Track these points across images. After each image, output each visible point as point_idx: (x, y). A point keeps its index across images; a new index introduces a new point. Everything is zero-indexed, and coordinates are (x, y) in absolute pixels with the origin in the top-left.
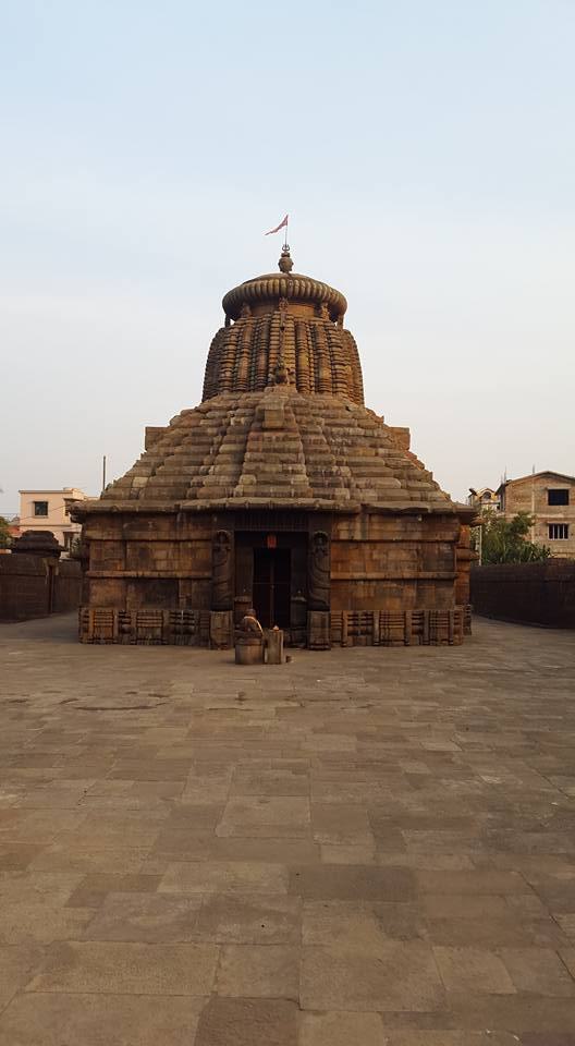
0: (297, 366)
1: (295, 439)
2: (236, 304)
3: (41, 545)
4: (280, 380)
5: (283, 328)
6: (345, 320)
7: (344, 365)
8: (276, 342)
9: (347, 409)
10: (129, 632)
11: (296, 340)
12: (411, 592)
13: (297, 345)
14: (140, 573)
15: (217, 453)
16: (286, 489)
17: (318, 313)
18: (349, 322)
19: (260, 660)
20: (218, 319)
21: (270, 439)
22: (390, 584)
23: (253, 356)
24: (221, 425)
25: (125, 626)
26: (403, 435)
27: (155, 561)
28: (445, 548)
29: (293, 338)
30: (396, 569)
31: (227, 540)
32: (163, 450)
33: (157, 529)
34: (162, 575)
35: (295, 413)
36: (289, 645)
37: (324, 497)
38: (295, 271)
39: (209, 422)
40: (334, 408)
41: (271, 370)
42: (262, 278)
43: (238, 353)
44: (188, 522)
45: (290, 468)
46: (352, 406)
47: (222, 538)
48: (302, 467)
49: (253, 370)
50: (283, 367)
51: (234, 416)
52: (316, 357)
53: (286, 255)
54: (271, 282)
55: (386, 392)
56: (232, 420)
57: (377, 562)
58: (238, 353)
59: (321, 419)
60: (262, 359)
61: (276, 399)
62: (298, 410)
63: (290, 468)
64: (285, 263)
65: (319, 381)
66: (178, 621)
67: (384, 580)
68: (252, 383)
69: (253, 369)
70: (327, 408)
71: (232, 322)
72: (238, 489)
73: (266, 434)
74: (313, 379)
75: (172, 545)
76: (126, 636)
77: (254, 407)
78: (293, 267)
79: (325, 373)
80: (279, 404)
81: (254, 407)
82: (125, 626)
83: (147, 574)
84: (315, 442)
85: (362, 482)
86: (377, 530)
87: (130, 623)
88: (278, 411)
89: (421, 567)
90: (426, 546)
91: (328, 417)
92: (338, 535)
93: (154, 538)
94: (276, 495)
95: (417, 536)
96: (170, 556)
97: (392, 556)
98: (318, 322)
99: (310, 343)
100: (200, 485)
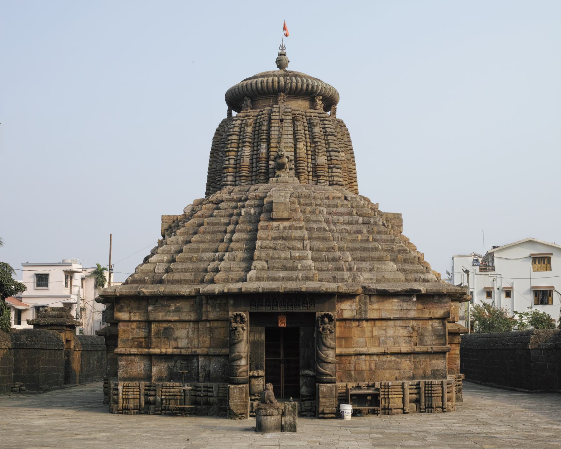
0: (296, 153)
1: (301, 228)
2: (236, 99)
3: (59, 321)
4: (281, 167)
5: (282, 120)
6: (337, 110)
7: (339, 152)
8: (277, 133)
9: (346, 198)
10: (154, 403)
11: (294, 130)
12: (406, 364)
13: (295, 134)
14: (164, 350)
15: (231, 241)
16: (294, 274)
17: (313, 106)
18: (342, 111)
20: (221, 111)
22: (389, 358)
24: (231, 215)
25: (151, 398)
26: (395, 220)
27: (176, 339)
28: (437, 324)
29: (292, 129)
30: (394, 344)
31: (242, 320)
32: (181, 239)
33: (178, 310)
34: (184, 351)
35: (299, 204)
36: (302, 414)
39: (222, 213)
40: (334, 198)
41: (272, 158)
42: (263, 76)
43: (241, 142)
44: (207, 303)
45: (297, 255)
46: (350, 195)
47: (239, 319)
48: (309, 254)
49: (255, 158)
50: (283, 156)
51: (243, 207)
52: (314, 145)
54: (270, 79)
55: (377, 180)
56: (243, 211)
57: (378, 338)
58: (241, 142)
59: (322, 208)
60: (263, 148)
61: (283, 190)
62: (302, 201)
63: (297, 255)
64: (281, 63)
65: (315, 167)
66: (198, 393)
67: (384, 354)
68: (254, 169)
69: (255, 157)
70: (328, 198)
71: (234, 114)
72: (252, 274)
73: (275, 224)
74: (310, 165)
75: (191, 324)
76: (150, 407)
77: (262, 199)
78: (289, 64)
79: (322, 160)
80: (286, 197)
81: (262, 199)
82: (151, 398)
83: (170, 351)
84: (319, 230)
85: (364, 265)
86: (376, 309)
87: (155, 395)
88: (285, 203)
89: (417, 341)
90: (420, 323)
91: (329, 206)
92: (342, 313)
93: (177, 318)
94: (283, 279)
95: (412, 314)
96: (191, 335)
97: (391, 332)
98: (313, 113)
99: (307, 132)
100: (217, 270)
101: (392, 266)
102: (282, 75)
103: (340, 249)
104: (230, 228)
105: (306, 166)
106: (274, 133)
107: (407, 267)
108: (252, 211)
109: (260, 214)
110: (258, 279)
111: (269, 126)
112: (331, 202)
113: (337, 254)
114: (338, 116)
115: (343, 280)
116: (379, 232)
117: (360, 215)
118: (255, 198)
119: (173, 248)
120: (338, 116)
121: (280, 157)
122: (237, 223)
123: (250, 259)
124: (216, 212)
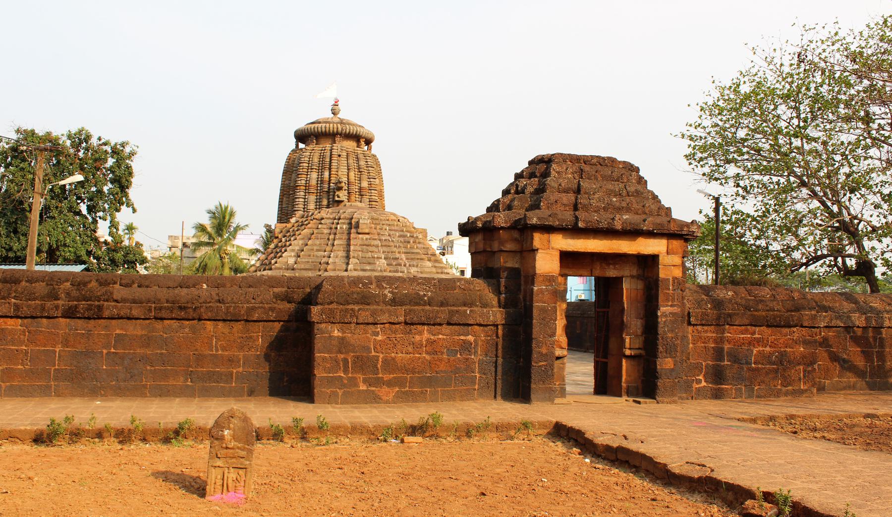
18: (375, 147)
20: (291, 143)
21: (362, 239)
23: (321, 170)
32: (301, 242)
37: (394, 272)
38: (341, 115)
39: (325, 226)
42: (326, 122)
53: (336, 104)
56: (339, 227)
58: (310, 168)
60: (327, 174)
65: (360, 189)
71: (301, 146)
73: (360, 236)
79: (365, 184)
98: (359, 151)
101: (429, 264)
102: (337, 123)
103: (399, 253)
104: (332, 237)
105: (355, 188)
106: (334, 164)
107: (437, 265)
108: (344, 227)
109: (350, 228)
110: (355, 270)
111: (331, 160)
112: (391, 223)
113: (398, 255)
114: (373, 151)
115: (403, 272)
116: (419, 243)
117: (408, 231)
118: (344, 219)
119: (297, 248)
120: (373, 151)
121: (340, 182)
122: (335, 234)
123: (348, 257)
124: (320, 226)
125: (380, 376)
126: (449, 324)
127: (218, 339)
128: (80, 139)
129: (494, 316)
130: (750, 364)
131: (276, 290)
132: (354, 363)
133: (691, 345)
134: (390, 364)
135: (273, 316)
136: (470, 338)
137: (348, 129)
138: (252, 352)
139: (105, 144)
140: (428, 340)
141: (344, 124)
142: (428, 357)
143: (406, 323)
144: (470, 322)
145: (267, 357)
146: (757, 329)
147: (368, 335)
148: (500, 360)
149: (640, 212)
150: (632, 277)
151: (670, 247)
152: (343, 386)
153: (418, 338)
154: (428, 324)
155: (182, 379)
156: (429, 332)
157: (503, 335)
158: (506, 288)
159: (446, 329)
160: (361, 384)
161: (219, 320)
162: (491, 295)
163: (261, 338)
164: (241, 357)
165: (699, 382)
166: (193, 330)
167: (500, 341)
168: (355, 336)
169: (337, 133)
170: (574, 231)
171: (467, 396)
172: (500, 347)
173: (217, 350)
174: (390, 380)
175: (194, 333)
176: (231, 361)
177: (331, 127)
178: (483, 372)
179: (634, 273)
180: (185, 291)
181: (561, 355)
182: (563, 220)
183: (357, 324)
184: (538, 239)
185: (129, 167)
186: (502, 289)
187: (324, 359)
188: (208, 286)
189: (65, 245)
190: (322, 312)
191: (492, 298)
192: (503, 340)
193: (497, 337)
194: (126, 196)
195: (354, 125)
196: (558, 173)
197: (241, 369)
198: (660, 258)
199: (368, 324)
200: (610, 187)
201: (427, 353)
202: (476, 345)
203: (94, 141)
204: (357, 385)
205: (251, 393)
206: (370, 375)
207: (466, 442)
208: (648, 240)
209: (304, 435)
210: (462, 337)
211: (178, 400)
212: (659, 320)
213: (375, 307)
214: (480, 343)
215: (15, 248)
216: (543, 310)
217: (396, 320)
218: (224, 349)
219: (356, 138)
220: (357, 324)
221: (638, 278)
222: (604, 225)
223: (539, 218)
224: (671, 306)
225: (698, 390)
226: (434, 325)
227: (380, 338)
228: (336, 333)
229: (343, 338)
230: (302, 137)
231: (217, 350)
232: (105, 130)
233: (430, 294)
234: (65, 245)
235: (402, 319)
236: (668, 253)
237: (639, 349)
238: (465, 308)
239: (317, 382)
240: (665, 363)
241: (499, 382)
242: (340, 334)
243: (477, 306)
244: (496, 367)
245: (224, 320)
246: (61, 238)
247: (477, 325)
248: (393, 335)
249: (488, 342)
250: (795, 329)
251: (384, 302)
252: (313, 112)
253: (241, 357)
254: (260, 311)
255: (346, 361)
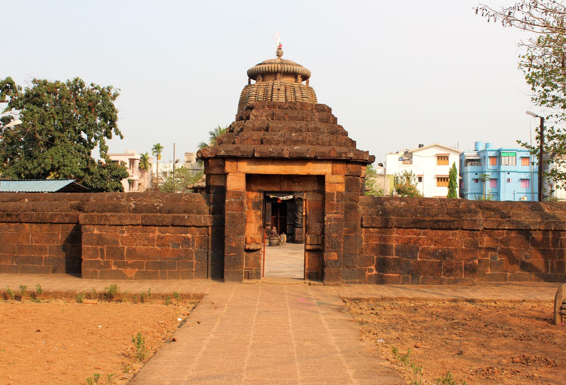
2: (252, 75)
5: (279, 90)
18: (312, 83)
19: (278, 245)
36: (288, 242)
42: (269, 63)
71: (253, 82)
98: (296, 85)
102: (279, 63)
111: (272, 93)
114: (310, 85)
120: (310, 85)
125: (126, 260)
126: (173, 225)
127: (33, 235)
128: (77, 85)
129: (205, 220)
130: (416, 258)
131: (72, 202)
132: (108, 251)
133: (364, 243)
134: (132, 253)
135: (67, 220)
136: (189, 235)
137: (287, 68)
138: (55, 244)
139: (96, 88)
140: (158, 237)
141: (284, 64)
142: (158, 248)
143: (143, 225)
144: (188, 224)
145: (64, 248)
146: (422, 231)
147: (118, 233)
148: (210, 252)
149: (314, 143)
150: (314, 191)
151: (334, 169)
152: (101, 267)
153: (151, 235)
154: (159, 226)
155: (10, 261)
156: (160, 231)
157: (212, 233)
158: (214, 200)
159: (171, 229)
160: (113, 266)
161: (33, 223)
162: (205, 205)
163: (61, 235)
164: (48, 247)
165: (371, 270)
166: (16, 228)
167: (210, 237)
168: (108, 233)
169: (278, 72)
170: (252, 159)
171: (187, 276)
172: (210, 242)
173: (32, 243)
174: (132, 264)
175: (17, 231)
176: (41, 250)
177: (273, 67)
178: (198, 259)
179: (316, 188)
180: (13, 203)
181: (255, 248)
182: (245, 152)
183: (110, 225)
184: (229, 166)
185: (111, 106)
186: (211, 200)
187: (88, 248)
188: (28, 200)
189: (64, 165)
190: (86, 217)
191: (206, 208)
192: (212, 237)
193: (209, 235)
194: (115, 126)
195: (292, 64)
196: (255, 116)
197: (48, 255)
198: (326, 178)
199: (117, 225)
200: (293, 125)
201: (158, 245)
202: (193, 240)
203: (88, 86)
204: (110, 267)
205: (54, 271)
206: (118, 260)
207: (141, 305)
208: (316, 165)
209: (33, 296)
210: (183, 235)
211: (6, 274)
212: (326, 224)
213: (122, 214)
214: (196, 239)
215: (29, 168)
216: (233, 216)
217: (136, 223)
218: (37, 242)
219: (294, 75)
220: (110, 225)
221: (318, 192)
222: (275, 154)
223: (226, 151)
224: (335, 213)
225: (370, 277)
226: (163, 226)
227: (125, 235)
228: (96, 232)
229: (100, 235)
230: (252, 75)
231: (32, 243)
232: (93, 78)
233: (161, 204)
234: (64, 165)
235: (139, 222)
236: (333, 174)
237: (318, 245)
238: (185, 215)
239: (83, 264)
240: (331, 256)
241: (210, 266)
242: (99, 232)
243: (194, 213)
244: (208, 256)
245: (37, 223)
246: (62, 160)
247: (193, 226)
248: (135, 233)
249: (202, 238)
250: (457, 232)
251: (129, 211)
252: (264, 55)
253: (48, 247)
254: (59, 217)
255: (102, 250)
